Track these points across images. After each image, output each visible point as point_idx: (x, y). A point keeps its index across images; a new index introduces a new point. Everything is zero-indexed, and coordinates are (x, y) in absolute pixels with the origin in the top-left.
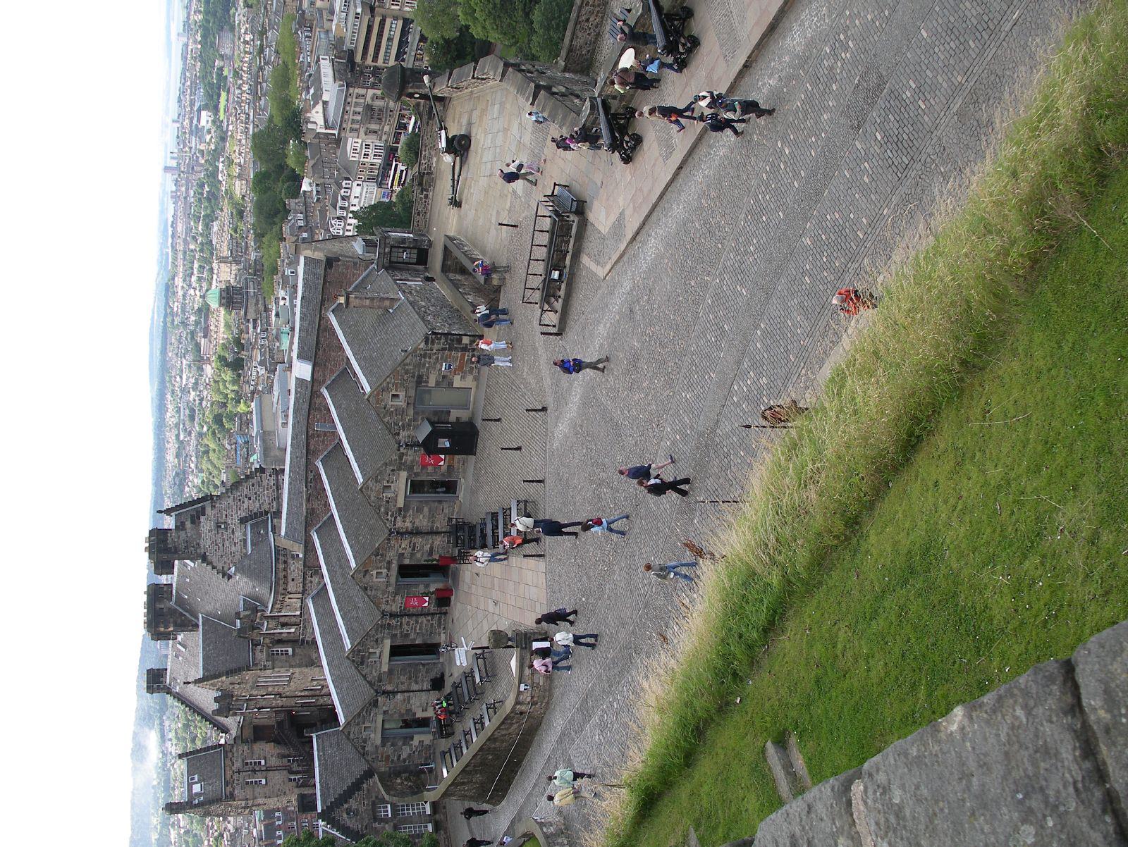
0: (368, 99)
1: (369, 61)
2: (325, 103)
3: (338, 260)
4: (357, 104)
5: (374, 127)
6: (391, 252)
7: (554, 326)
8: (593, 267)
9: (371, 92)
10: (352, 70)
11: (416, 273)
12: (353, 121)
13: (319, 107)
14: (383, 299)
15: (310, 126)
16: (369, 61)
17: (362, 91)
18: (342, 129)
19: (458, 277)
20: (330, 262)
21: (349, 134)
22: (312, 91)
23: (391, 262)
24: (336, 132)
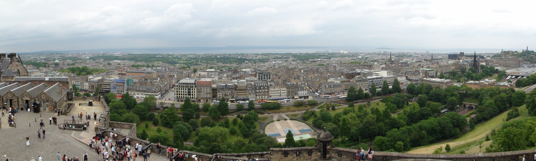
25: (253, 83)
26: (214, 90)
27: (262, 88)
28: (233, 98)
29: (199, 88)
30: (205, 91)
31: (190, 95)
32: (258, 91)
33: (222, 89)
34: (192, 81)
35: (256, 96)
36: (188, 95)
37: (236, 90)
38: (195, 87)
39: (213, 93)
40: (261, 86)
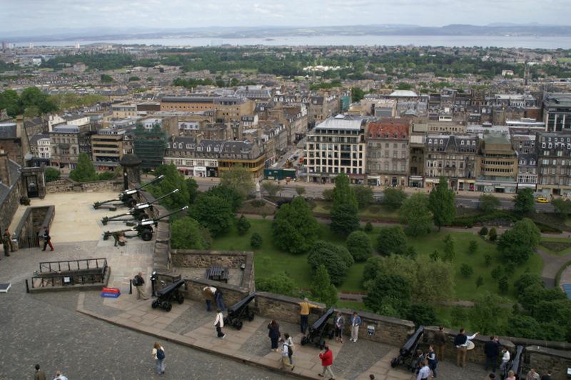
0: (73, 146)
1: (94, 143)
2: (66, 123)
3: (20, 145)
4: (69, 140)
5: (58, 150)
6: (32, 176)
7: (33, 287)
8: (80, 302)
9: (77, 146)
10: (87, 135)
11: (22, 193)
12: (59, 139)
13: (62, 120)
14: (7, 176)
15: (51, 117)
16: (94, 143)
17: (76, 141)
18: (54, 134)
19: (31, 219)
20: (18, 141)
21: (51, 138)
22: (70, 115)
23: (26, 177)
24: (51, 130)
25: (533, 138)
26: (416, 151)
27: (560, 154)
28: (469, 177)
29: (375, 144)
30: (391, 155)
31: (348, 163)
32: (546, 162)
33: (441, 150)
34: (355, 125)
35: (541, 175)
36: (344, 163)
37: (481, 153)
38: (363, 140)
39: (413, 159)
40: (559, 148)
